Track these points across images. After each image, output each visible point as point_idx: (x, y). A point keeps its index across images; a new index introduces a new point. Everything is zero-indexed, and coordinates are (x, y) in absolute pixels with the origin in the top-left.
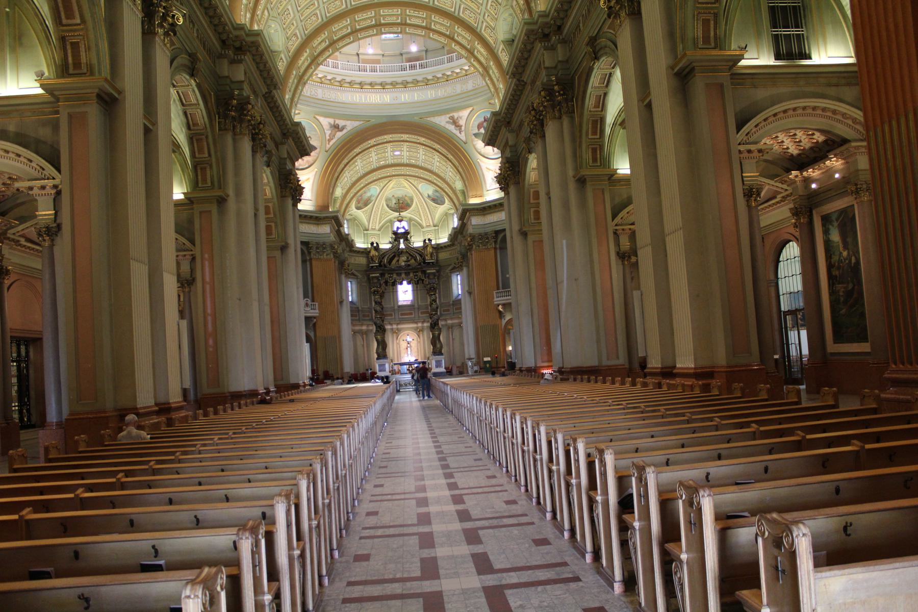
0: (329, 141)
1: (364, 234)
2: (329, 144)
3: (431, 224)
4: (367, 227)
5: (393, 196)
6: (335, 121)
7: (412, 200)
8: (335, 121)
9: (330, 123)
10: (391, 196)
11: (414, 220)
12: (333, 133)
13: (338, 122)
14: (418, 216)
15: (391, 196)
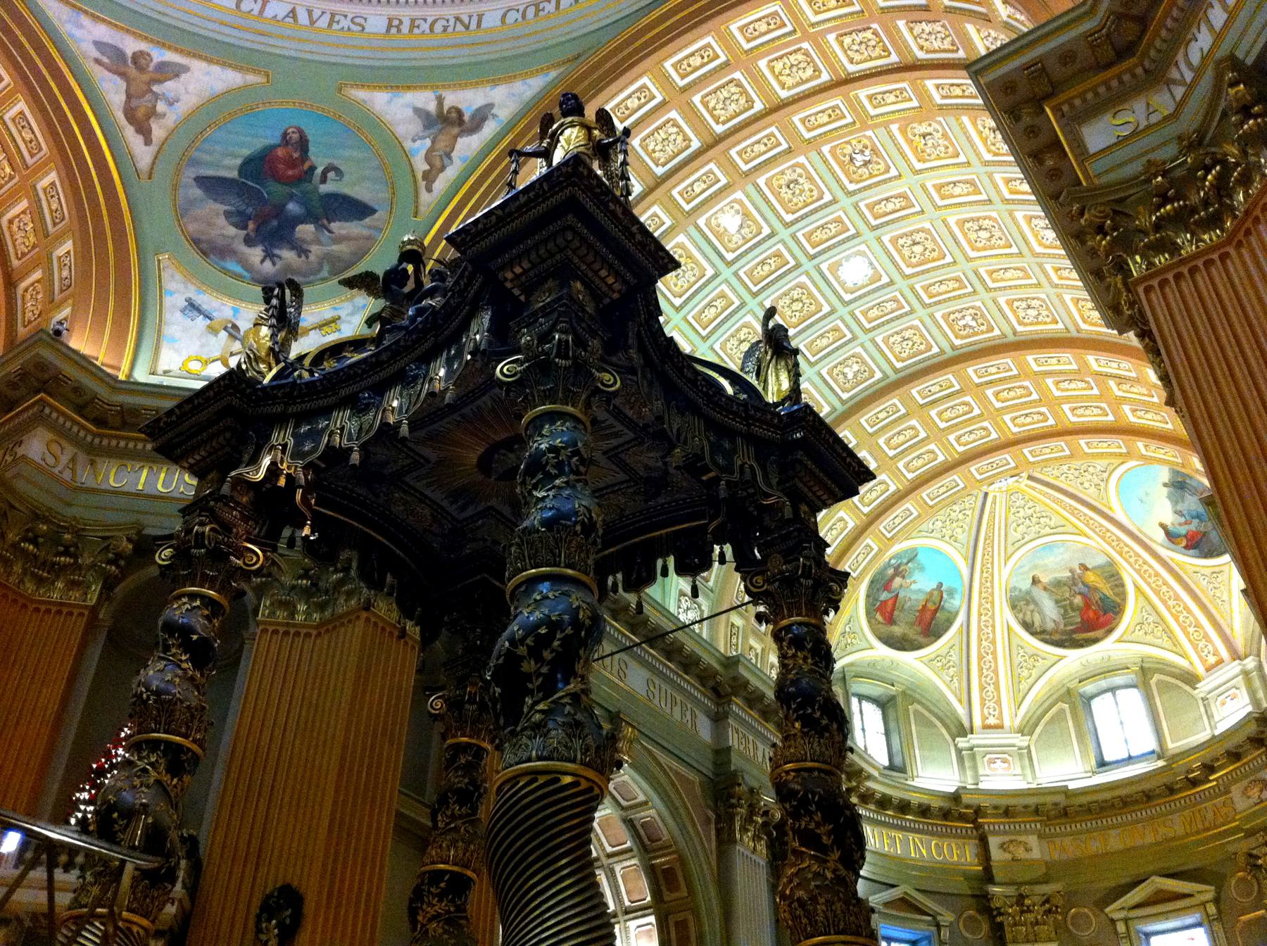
0: (429, 177)
1: (959, 751)
2: (429, 190)
3: (1225, 654)
4: (966, 724)
5: (1035, 581)
6: (440, 101)
7: (1114, 577)
8: (440, 101)
9: (417, 111)
10: (1025, 584)
11: (1164, 668)
12: (441, 145)
13: (452, 99)
14: (1168, 644)
15: (1025, 584)
